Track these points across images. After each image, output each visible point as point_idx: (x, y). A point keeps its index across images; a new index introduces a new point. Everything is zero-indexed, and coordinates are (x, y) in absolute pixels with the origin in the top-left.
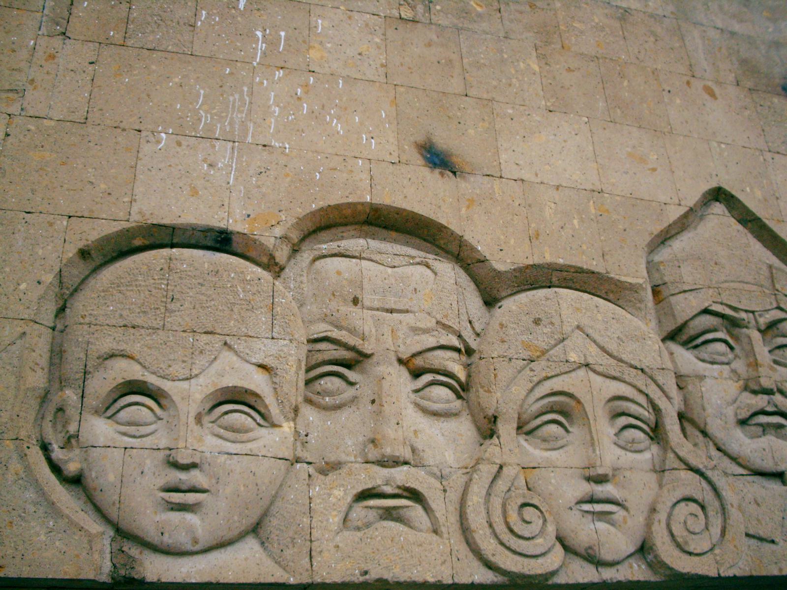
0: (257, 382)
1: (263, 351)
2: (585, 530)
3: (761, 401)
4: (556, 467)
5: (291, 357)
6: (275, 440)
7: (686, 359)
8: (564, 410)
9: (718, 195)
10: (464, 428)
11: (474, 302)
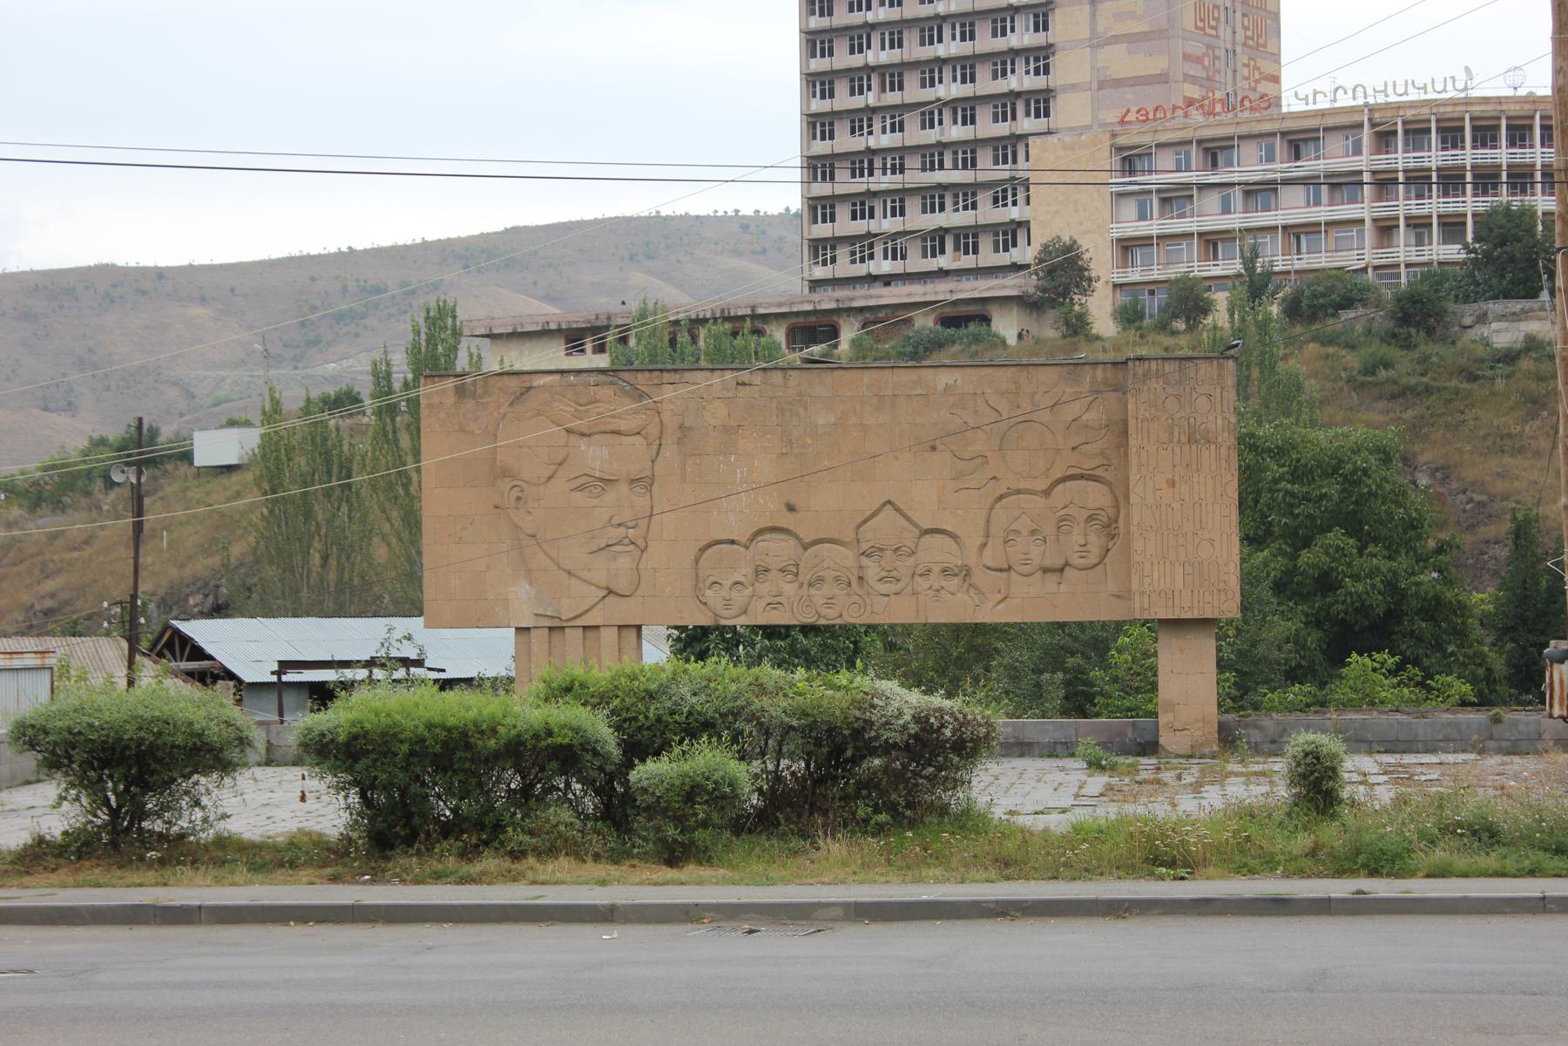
0: (742, 579)
1: (744, 571)
2: (824, 611)
3: (884, 574)
4: (819, 596)
5: (749, 571)
6: (748, 592)
7: (865, 561)
8: (821, 580)
9: (889, 502)
10: (796, 585)
11: (800, 550)
